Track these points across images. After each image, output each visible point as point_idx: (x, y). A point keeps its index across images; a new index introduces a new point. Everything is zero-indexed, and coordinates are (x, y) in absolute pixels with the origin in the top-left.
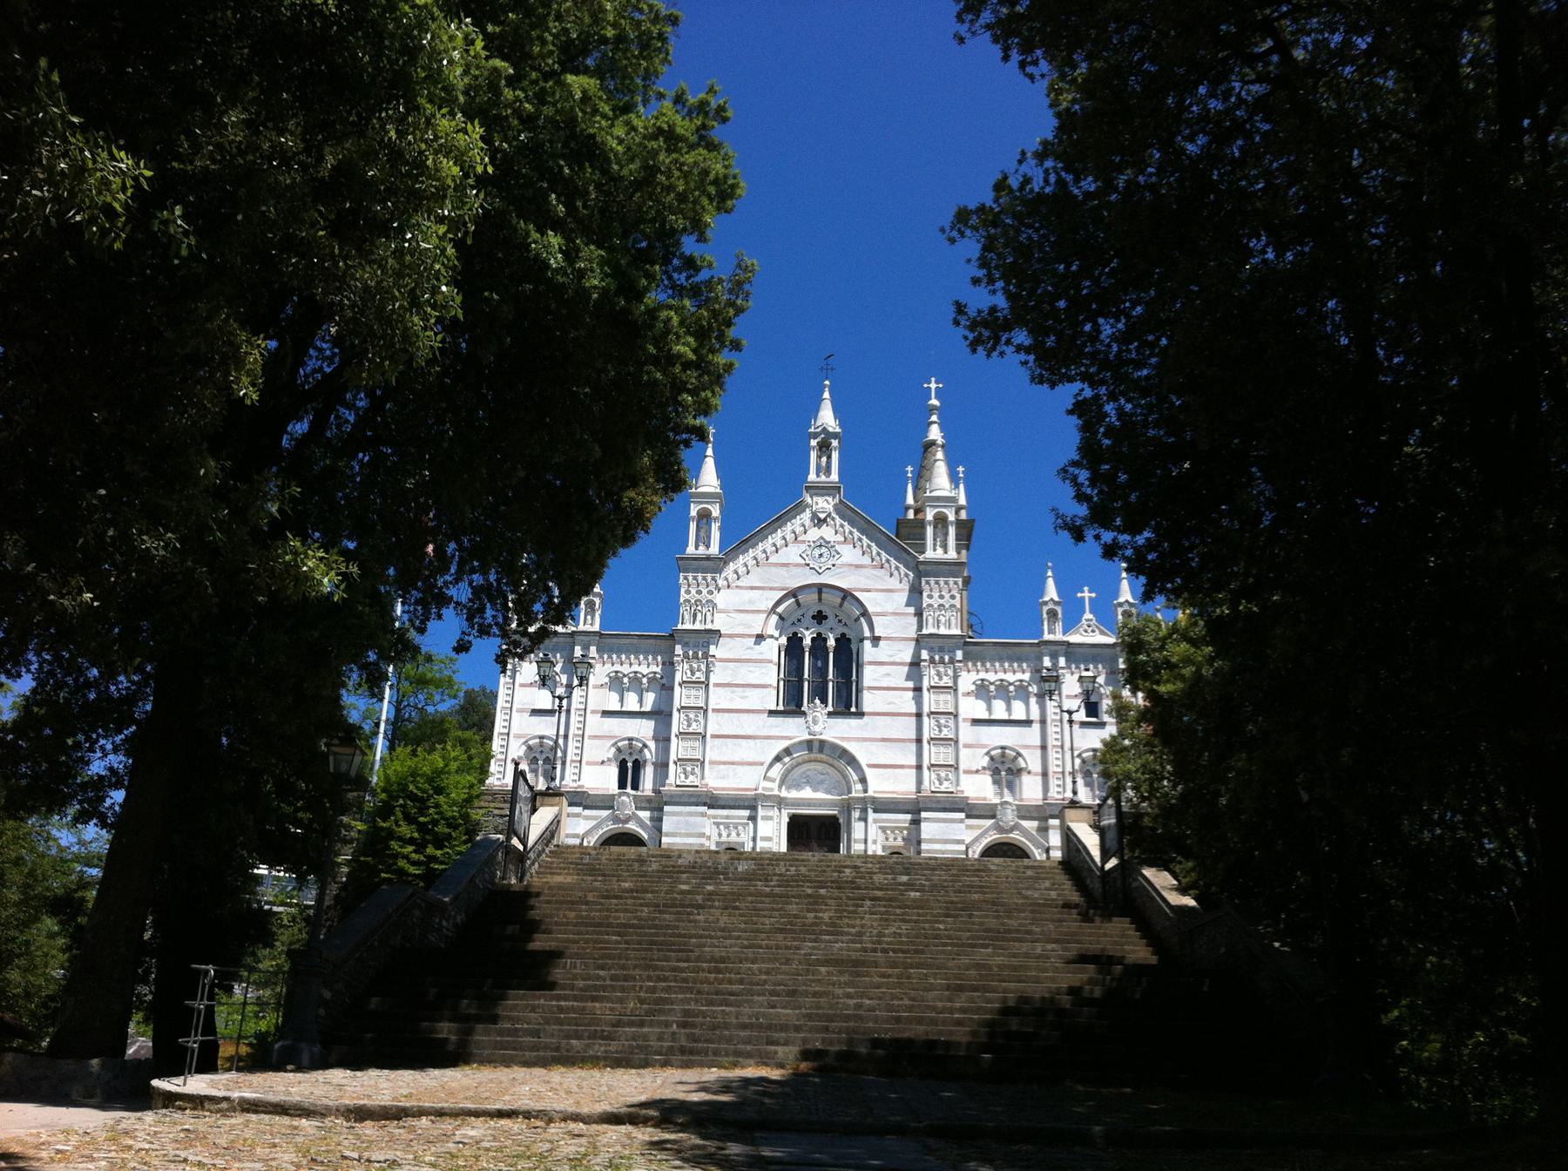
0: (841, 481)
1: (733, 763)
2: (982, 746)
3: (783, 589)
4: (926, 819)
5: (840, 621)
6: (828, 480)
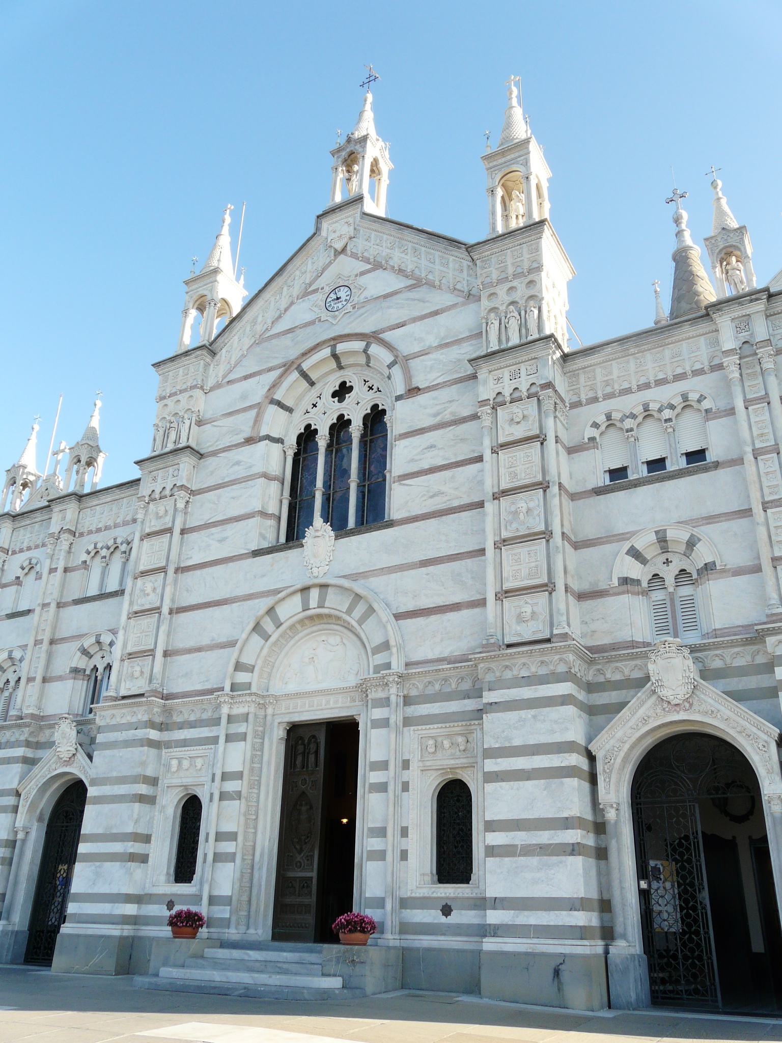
1: (199, 649)
2: (622, 537)
4: (493, 707)
5: (371, 388)
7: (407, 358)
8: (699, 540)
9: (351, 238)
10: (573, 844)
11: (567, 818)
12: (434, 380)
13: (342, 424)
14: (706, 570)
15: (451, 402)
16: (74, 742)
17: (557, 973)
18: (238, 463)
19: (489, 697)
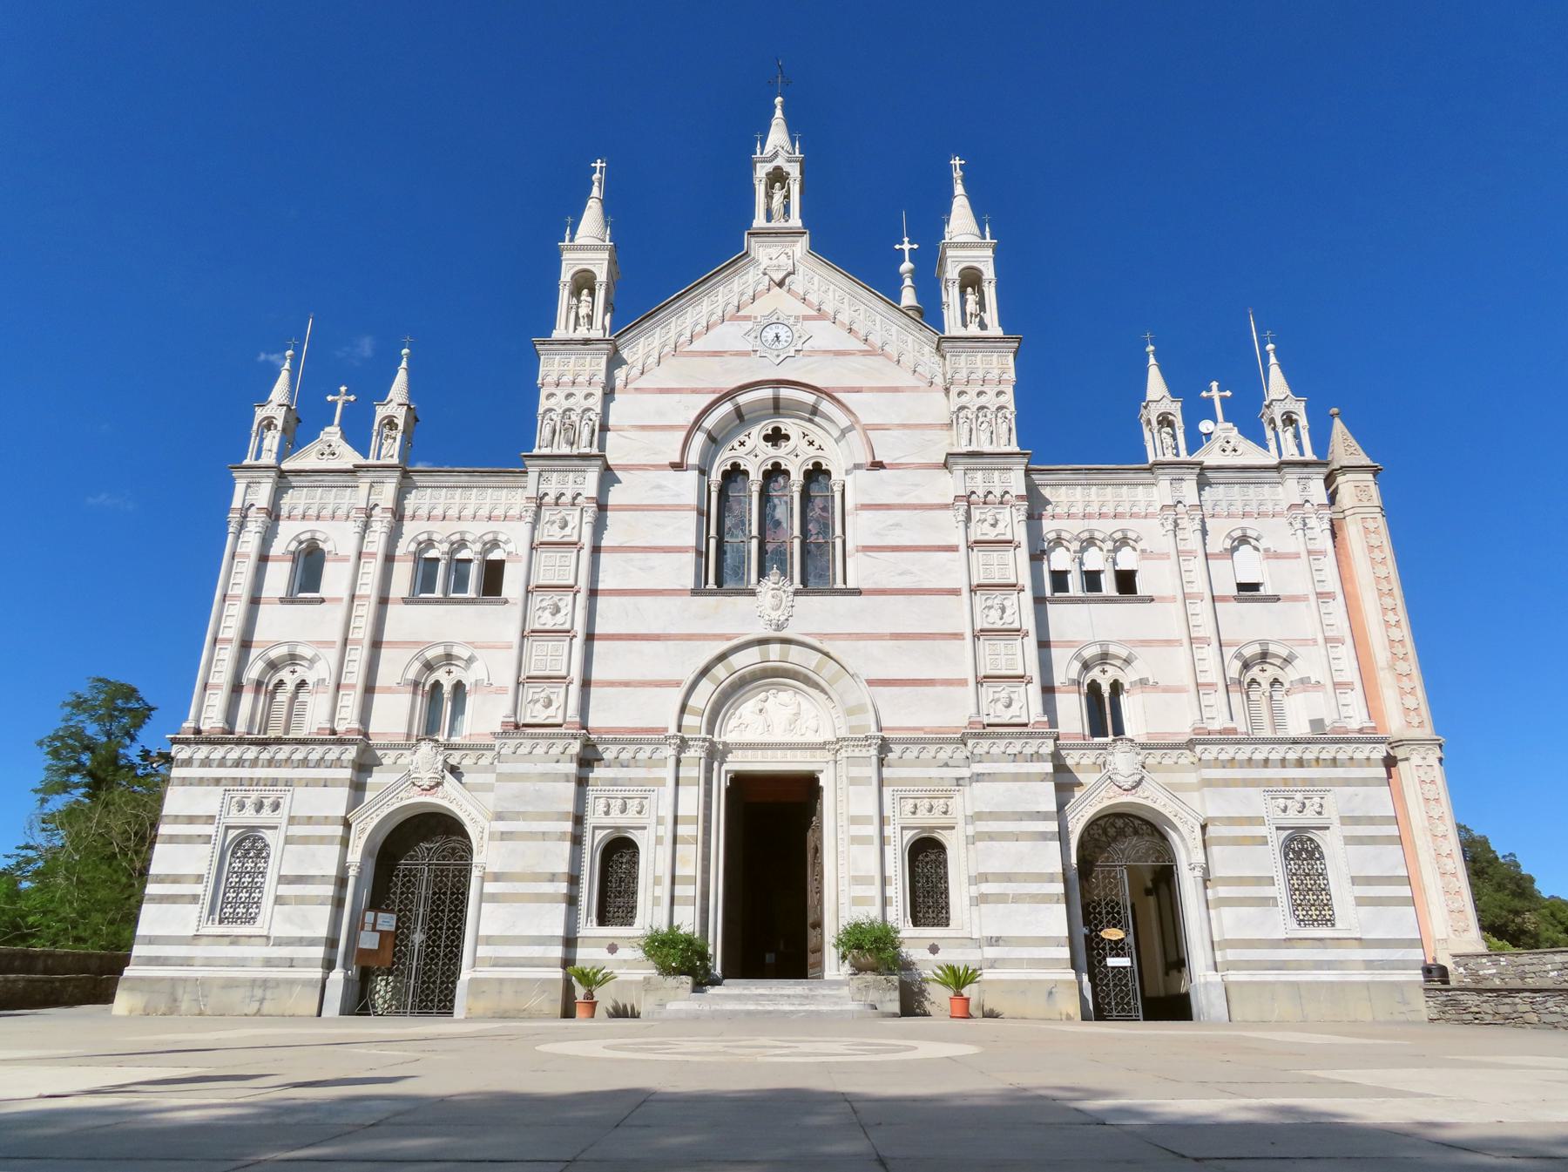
0: (805, 225)
1: (626, 684)
2: (1068, 644)
3: (714, 392)
5: (811, 443)
6: (786, 225)
7: (866, 428)
8: (1136, 658)
9: (789, 274)
10: (1058, 894)
11: (1052, 874)
12: (895, 460)
13: (775, 472)
14: (1141, 683)
15: (917, 485)
16: (440, 768)
17: (1050, 993)
18: (659, 487)
19: (977, 768)
